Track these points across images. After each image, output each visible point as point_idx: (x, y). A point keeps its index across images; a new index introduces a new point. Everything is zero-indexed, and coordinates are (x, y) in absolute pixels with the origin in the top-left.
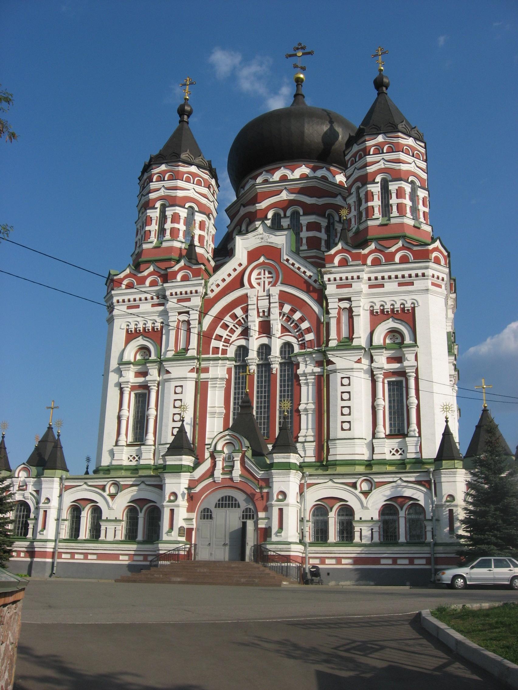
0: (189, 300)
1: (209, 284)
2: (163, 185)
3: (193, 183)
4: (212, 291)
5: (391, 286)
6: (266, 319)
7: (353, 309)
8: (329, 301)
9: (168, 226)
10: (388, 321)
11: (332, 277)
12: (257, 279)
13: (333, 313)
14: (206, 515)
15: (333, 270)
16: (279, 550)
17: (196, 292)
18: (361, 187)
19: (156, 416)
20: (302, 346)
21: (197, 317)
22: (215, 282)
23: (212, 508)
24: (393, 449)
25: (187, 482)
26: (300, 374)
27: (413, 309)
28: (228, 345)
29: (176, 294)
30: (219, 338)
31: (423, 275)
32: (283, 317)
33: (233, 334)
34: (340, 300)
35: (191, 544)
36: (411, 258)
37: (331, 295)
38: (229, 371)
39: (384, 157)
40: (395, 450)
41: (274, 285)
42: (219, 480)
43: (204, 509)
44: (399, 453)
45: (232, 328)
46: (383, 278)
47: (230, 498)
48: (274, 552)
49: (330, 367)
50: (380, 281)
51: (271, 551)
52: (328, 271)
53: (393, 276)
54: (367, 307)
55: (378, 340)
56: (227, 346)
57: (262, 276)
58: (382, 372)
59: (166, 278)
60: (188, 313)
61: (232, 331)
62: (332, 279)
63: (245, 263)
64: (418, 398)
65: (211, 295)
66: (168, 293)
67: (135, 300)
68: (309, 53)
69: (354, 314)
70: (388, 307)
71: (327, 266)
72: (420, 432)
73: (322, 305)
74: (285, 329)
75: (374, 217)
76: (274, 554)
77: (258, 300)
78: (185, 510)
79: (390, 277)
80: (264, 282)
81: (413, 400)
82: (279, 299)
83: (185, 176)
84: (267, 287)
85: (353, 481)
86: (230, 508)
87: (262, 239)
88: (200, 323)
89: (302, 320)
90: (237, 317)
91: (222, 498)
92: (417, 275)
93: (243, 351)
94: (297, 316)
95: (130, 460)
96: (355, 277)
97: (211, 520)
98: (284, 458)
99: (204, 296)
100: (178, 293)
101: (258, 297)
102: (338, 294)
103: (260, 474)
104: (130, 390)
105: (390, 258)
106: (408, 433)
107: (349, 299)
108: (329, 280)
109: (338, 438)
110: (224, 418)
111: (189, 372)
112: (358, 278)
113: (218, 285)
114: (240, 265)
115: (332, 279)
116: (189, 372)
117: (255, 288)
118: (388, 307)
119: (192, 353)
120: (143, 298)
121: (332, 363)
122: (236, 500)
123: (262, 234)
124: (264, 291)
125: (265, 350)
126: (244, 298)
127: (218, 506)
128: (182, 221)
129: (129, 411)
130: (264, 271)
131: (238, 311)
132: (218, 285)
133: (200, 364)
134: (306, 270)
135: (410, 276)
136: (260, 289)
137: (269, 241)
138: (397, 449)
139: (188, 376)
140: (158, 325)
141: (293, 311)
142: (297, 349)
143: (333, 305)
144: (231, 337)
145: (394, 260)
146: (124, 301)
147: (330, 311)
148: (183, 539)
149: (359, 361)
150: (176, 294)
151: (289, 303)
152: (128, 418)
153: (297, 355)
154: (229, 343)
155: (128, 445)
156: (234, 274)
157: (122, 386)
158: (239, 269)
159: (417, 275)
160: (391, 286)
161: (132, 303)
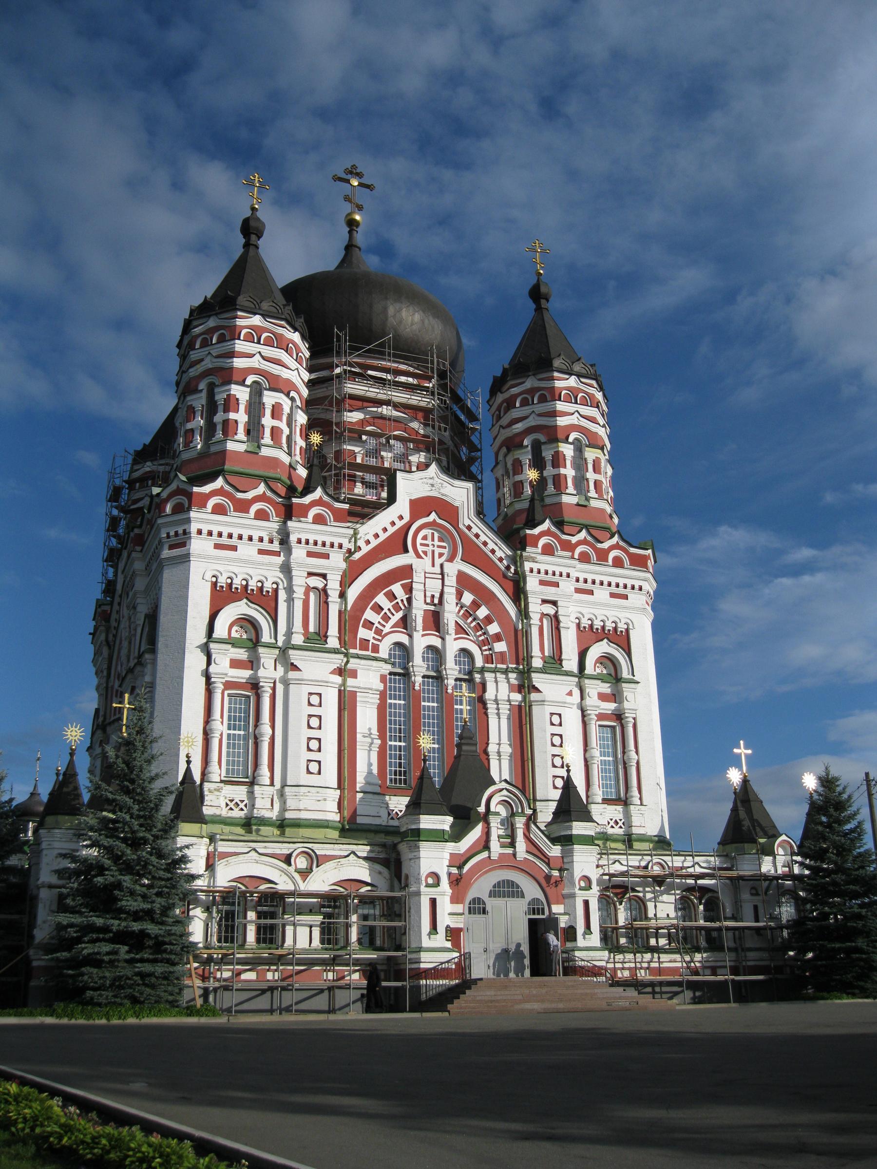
0: (326, 556)
1: (358, 537)
2: (258, 350)
3: (296, 360)
4: (360, 548)
5: (602, 594)
6: (432, 608)
7: (561, 618)
8: (530, 600)
9: (267, 421)
10: (601, 643)
11: (535, 566)
12: (422, 545)
13: (535, 619)
14: (478, 908)
15: (541, 558)
16: (590, 959)
17: (341, 546)
18: (544, 443)
19: (273, 738)
20: (488, 659)
21: (337, 586)
22: (363, 536)
23: (485, 897)
24: (611, 820)
25: (448, 856)
26: (489, 700)
27: (627, 630)
28: (380, 638)
29: (307, 542)
30: (369, 625)
31: (640, 589)
32: (459, 611)
33: (387, 622)
34: (544, 601)
35: (460, 952)
36: (626, 562)
37: (534, 593)
38: (383, 679)
39: (579, 410)
40: (613, 821)
41: (451, 559)
42: (494, 856)
43: (474, 899)
44: (619, 826)
45: (385, 613)
46: (594, 582)
47: (511, 884)
48: (588, 961)
49: (534, 696)
50: (589, 586)
51: (584, 961)
52: (532, 557)
53: (606, 583)
54: (573, 618)
55: (589, 669)
56: (378, 640)
57: (429, 542)
58: (597, 713)
59: (288, 512)
60: (324, 576)
61: (386, 618)
62: (535, 570)
63: (407, 518)
64: (637, 753)
65: (357, 556)
66: (293, 538)
67: (230, 536)
68: (368, 187)
69: (562, 625)
70: (598, 624)
71: (528, 549)
72: (641, 799)
73: (518, 606)
74: (460, 629)
75: (568, 491)
76: (589, 964)
77: (425, 577)
78: (447, 899)
79: (602, 583)
80: (433, 552)
81: (633, 754)
82: (458, 582)
83: (290, 345)
84: (438, 562)
85: (643, 864)
86: (511, 899)
87: (432, 485)
88: (342, 595)
89: (488, 620)
90: (396, 598)
91: (499, 883)
92: (633, 588)
93: (404, 652)
94: (483, 612)
95: (228, 807)
96: (564, 574)
97: (484, 916)
98: (585, 828)
99: (348, 557)
100: (311, 541)
101: (425, 573)
102: (542, 593)
103: (555, 851)
104: (223, 687)
105: (602, 556)
106: (627, 799)
107: (554, 603)
108: (531, 571)
109: (550, 799)
110: (378, 752)
111: (330, 673)
112: (568, 576)
113: (368, 542)
114: (401, 518)
115: (535, 570)
116: (331, 673)
117: (421, 557)
118: (598, 624)
119: (333, 642)
120: (245, 537)
121: (537, 690)
122: (518, 887)
123: (432, 478)
124: (433, 565)
125: (436, 655)
126: (406, 572)
127: (493, 894)
128: (285, 418)
129: (222, 723)
130: (433, 534)
131: (397, 589)
132: (368, 542)
133: (348, 662)
134: (496, 548)
135: (625, 587)
136: (428, 560)
137: (442, 491)
138: (616, 821)
139: (331, 680)
140: (268, 586)
141: (476, 605)
142: (479, 662)
143: (535, 608)
144: (384, 626)
145: (607, 562)
146: (210, 533)
147: (531, 614)
148: (448, 945)
149: (570, 694)
150: (307, 542)
151: (472, 591)
152: (221, 735)
153: (482, 671)
154: (380, 635)
155: (222, 781)
156: (391, 530)
157: (213, 680)
158: (399, 524)
159: (633, 588)
160: (602, 594)
161: (224, 540)
